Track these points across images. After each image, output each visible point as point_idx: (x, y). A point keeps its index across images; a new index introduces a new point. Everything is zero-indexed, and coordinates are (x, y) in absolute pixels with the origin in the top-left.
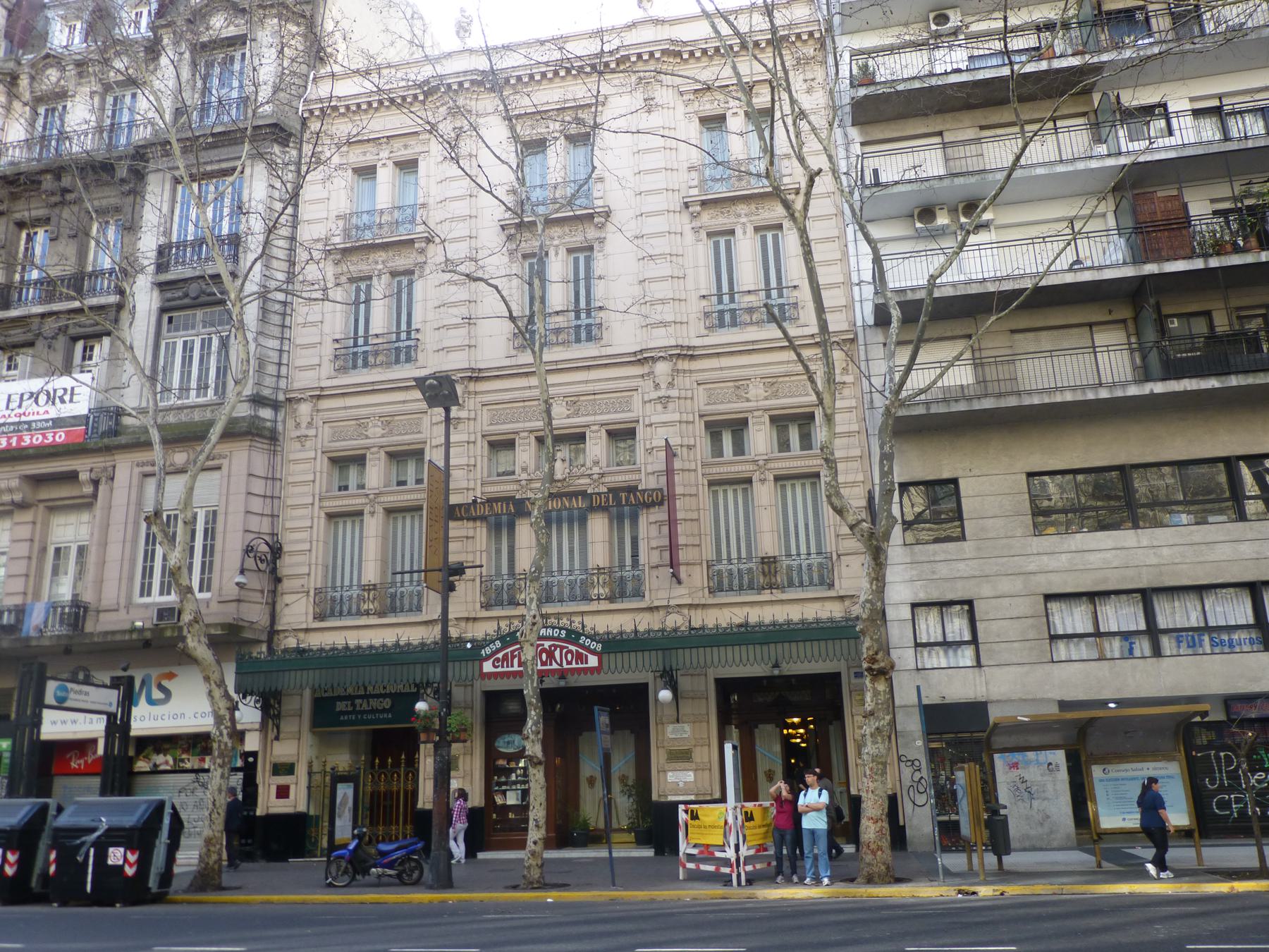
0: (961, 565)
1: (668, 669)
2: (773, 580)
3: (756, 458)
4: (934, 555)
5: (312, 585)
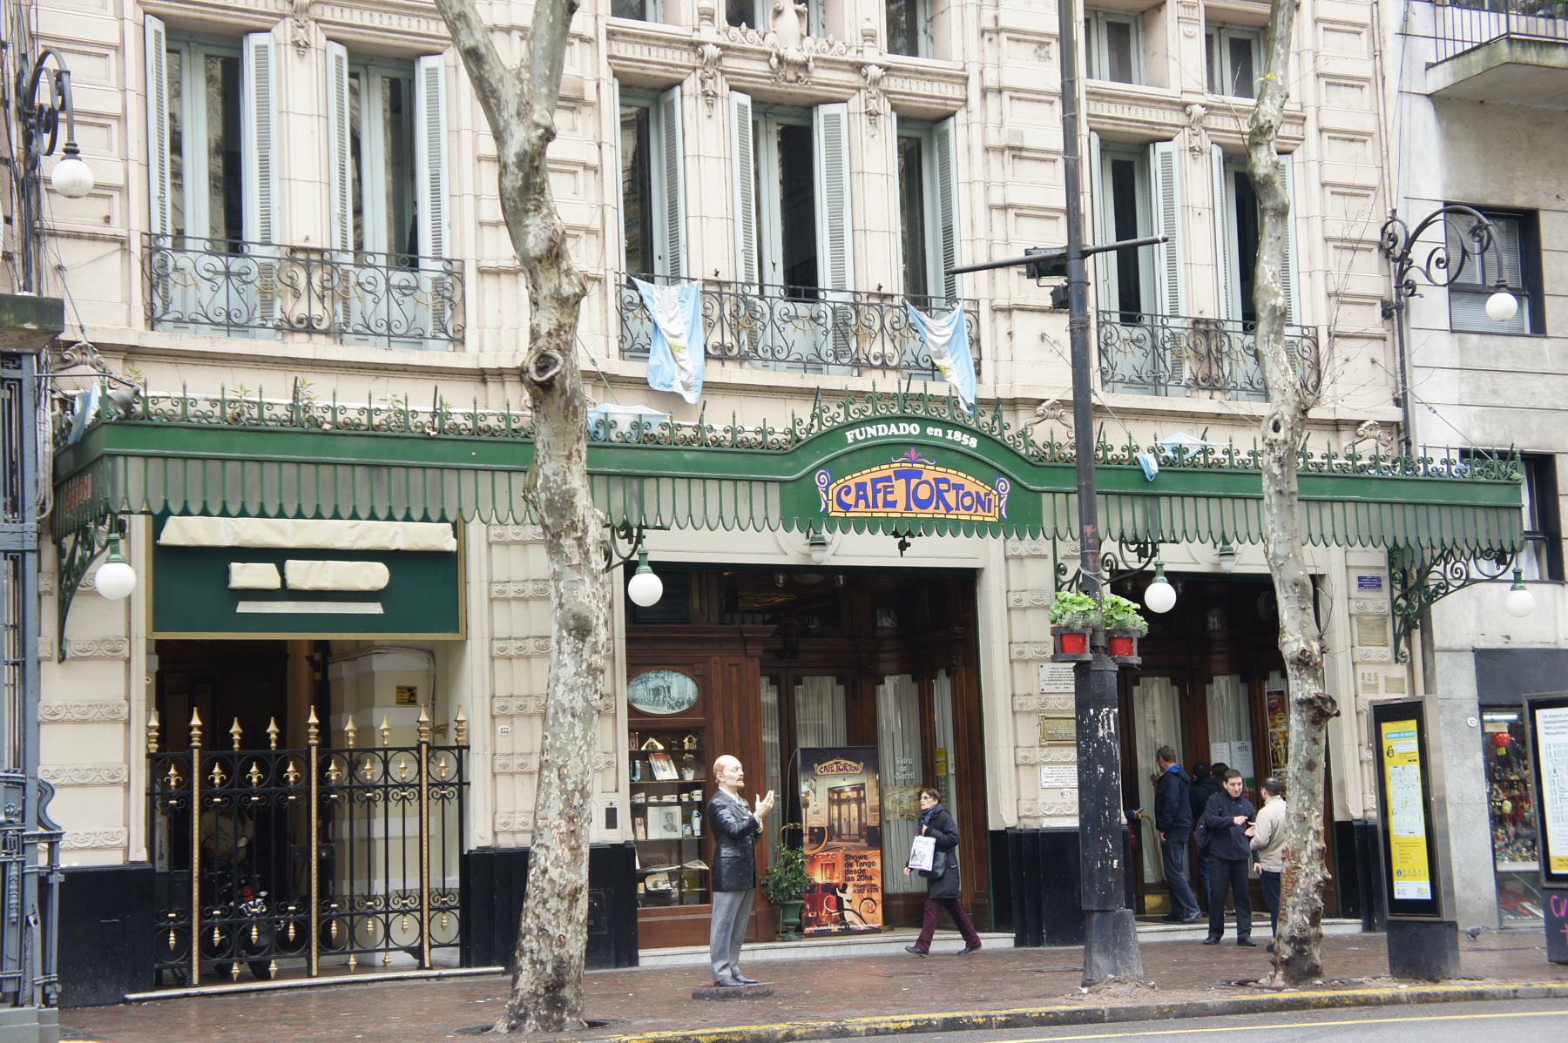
0: (1537, 384)
1: (1401, 544)
2: (1215, 370)
3: (1186, 98)
4: (1496, 357)
5: (137, 224)
